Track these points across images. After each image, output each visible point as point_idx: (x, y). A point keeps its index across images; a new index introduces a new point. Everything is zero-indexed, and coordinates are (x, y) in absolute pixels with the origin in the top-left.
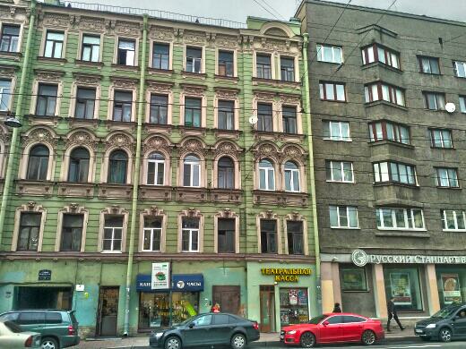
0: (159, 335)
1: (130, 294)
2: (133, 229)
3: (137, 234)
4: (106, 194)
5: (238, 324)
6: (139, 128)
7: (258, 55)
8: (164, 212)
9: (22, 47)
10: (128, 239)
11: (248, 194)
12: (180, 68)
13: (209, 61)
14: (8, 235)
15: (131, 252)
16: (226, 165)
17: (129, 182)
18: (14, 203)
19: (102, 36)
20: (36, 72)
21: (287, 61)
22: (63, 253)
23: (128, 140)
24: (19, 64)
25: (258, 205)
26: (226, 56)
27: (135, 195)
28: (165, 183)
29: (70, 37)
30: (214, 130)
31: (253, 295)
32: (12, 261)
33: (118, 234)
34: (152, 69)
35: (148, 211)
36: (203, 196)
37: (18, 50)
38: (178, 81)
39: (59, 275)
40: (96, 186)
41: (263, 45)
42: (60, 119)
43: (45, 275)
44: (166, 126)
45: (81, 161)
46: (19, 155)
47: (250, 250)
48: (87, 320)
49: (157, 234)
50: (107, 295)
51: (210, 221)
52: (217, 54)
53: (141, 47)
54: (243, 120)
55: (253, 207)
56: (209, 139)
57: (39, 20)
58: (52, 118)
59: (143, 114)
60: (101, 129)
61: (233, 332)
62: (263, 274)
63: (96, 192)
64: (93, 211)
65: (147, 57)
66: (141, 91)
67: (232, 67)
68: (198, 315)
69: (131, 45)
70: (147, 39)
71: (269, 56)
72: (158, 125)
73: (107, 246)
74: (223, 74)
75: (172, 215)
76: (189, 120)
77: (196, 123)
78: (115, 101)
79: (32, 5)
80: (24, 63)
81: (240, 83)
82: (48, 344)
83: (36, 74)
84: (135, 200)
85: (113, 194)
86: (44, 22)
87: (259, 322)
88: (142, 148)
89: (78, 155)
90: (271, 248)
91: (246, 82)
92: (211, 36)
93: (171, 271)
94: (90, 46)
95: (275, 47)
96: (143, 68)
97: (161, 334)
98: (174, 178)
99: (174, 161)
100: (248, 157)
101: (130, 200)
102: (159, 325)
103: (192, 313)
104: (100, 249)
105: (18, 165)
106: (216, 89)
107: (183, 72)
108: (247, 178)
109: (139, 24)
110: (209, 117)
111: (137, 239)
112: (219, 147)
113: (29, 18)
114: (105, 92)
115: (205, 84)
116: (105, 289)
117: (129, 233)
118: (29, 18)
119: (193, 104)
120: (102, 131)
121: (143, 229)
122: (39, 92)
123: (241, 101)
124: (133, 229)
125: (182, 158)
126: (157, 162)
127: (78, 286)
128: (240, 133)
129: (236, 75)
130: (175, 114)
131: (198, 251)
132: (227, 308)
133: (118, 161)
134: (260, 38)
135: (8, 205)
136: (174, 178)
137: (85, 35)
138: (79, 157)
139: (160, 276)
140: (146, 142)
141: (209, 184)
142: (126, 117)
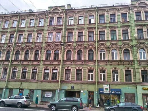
0: (107, 108)
1: (97, 94)
2: (96, 74)
3: (98, 75)
4: (88, 63)
5: (135, 106)
6: (96, 42)
7: (136, 13)
8: (106, 68)
9: (63, 23)
10: (95, 77)
11: (135, 61)
12: (108, 21)
13: (118, 18)
14: (62, 76)
15: (96, 81)
16: (127, 51)
17: (94, 59)
18: (63, 67)
19: (84, 16)
20: (66, 29)
21: (59, 18)
22: (77, 81)
23: (93, 46)
24: (62, 28)
25: (140, 65)
26: (124, 15)
27: (96, 63)
28: (106, 59)
29: (36, 20)
30: (121, 40)
31: (139, 97)
32: (64, 83)
33: (92, 75)
34: (100, 23)
35: (101, 68)
36: (119, 63)
37: (62, 24)
38: (108, 26)
39: (76, 88)
40: (85, 61)
41: (138, 9)
42: (74, 42)
43: (73, 87)
44: (105, 41)
45: (80, 54)
46: (64, 53)
47: (138, 81)
48: (85, 102)
49: (104, 75)
50: (90, 94)
51: (122, 71)
52: (121, 15)
53: (95, 17)
54: (132, 36)
55: (138, 66)
56: (120, 44)
57: (66, 14)
58: (72, 42)
59: (97, 38)
60: (85, 44)
61: (133, 109)
62: (142, 89)
63: (20, 62)
64: (84, 68)
65: (98, 20)
66: (96, 31)
67: (126, 18)
68: (120, 102)
69: (93, 17)
70: (97, 14)
71: (140, 12)
72: (102, 41)
73: (89, 79)
74: (123, 21)
75: (109, 69)
76: (112, 38)
77: (115, 39)
78: (89, 35)
79: (64, 10)
80: (63, 28)
81: (130, 23)
82: (53, 107)
83: (67, 30)
84: (96, 65)
85: (90, 63)
86: (68, 15)
87: (143, 106)
88: (97, 49)
89: (79, 52)
90: (146, 81)
91: (132, 23)
92: (118, 9)
93: (110, 88)
94: (81, 19)
95: (142, 9)
96: (96, 23)
97: (108, 108)
98: (85, 57)
99: (108, 52)
100: (135, 48)
101: (95, 65)
102: (107, 105)
103: (118, 102)
104: (87, 80)
105: (64, 56)
106: (121, 27)
107: (109, 23)
108: (135, 56)
109: (94, 10)
110: (119, 36)
111: (98, 77)
112: (123, 46)
113: (64, 14)
114: (86, 32)
115: (117, 25)
116: (89, 92)
117: (95, 75)
118: (64, 14)
119: (113, 32)
120: (85, 44)
121: (100, 74)
122: (78, 34)
123: (131, 29)
124: (96, 74)
125: (111, 50)
126: (102, 52)
127: (81, 91)
128: (131, 40)
129: (128, 21)
130: (108, 36)
131: (118, 81)
132: (130, 101)
133: (91, 53)
134: (136, 7)
135: (62, 67)
136: (85, 57)
137: (79, 16)
138: (79, 53)
139: (106, 89)
140: (15, 48)
141: (121, 59)
142: (92, 39)
